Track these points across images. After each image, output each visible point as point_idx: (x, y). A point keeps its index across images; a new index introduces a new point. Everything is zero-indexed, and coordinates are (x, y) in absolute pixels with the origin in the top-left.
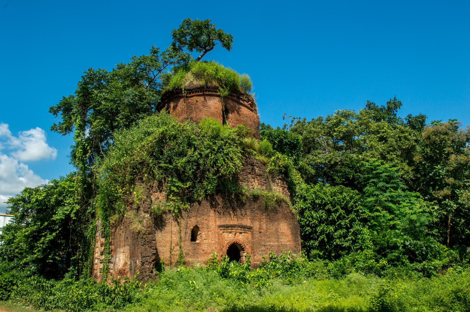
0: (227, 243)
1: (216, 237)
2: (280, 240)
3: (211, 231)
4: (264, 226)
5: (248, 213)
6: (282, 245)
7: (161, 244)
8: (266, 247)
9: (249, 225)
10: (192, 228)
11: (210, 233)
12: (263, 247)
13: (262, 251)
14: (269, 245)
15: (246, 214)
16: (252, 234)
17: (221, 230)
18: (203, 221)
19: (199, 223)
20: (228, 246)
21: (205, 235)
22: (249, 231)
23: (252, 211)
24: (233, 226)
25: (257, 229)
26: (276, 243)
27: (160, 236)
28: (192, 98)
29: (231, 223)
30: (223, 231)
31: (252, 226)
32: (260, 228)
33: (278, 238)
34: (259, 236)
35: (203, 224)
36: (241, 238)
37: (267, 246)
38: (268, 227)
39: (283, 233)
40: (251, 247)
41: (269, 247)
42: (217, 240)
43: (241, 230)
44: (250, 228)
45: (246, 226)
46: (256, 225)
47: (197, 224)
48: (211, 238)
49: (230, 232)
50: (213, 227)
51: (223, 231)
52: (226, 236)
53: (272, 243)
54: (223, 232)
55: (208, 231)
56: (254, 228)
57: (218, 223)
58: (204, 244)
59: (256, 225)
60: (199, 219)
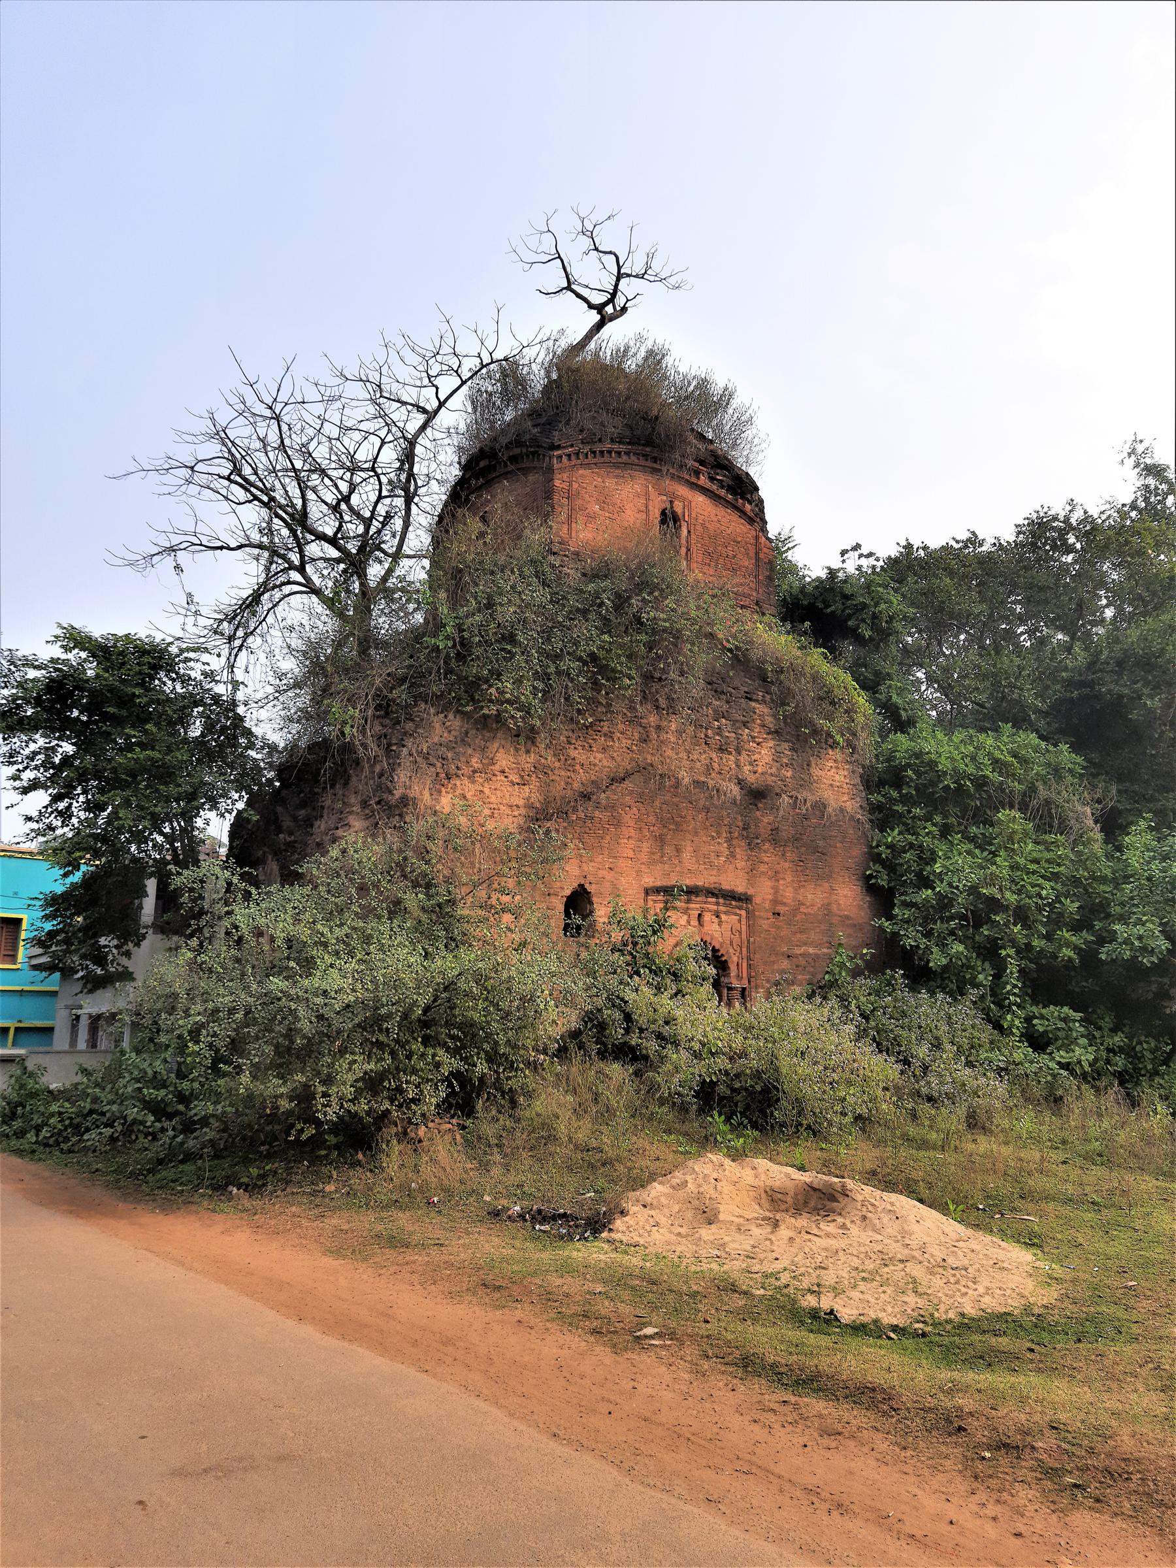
9: (740, 889)
10: (568, 892)
15: (732, 855)
17: (655, 901)
18: (601, 873)
19: (590, 878)
24: (692, 891)
26: (825, 950)
32: (775, 902)
37: (796, 956)
40: (749, 959)
41: (802, 961)
43: (717, 904)
45: (733, 891)
46: (762, 893)
49: (686, 911)
50: (630, 892)
53: (811, 950)
56: (757, 900)
57: (649, 881)
60: (589, 868)
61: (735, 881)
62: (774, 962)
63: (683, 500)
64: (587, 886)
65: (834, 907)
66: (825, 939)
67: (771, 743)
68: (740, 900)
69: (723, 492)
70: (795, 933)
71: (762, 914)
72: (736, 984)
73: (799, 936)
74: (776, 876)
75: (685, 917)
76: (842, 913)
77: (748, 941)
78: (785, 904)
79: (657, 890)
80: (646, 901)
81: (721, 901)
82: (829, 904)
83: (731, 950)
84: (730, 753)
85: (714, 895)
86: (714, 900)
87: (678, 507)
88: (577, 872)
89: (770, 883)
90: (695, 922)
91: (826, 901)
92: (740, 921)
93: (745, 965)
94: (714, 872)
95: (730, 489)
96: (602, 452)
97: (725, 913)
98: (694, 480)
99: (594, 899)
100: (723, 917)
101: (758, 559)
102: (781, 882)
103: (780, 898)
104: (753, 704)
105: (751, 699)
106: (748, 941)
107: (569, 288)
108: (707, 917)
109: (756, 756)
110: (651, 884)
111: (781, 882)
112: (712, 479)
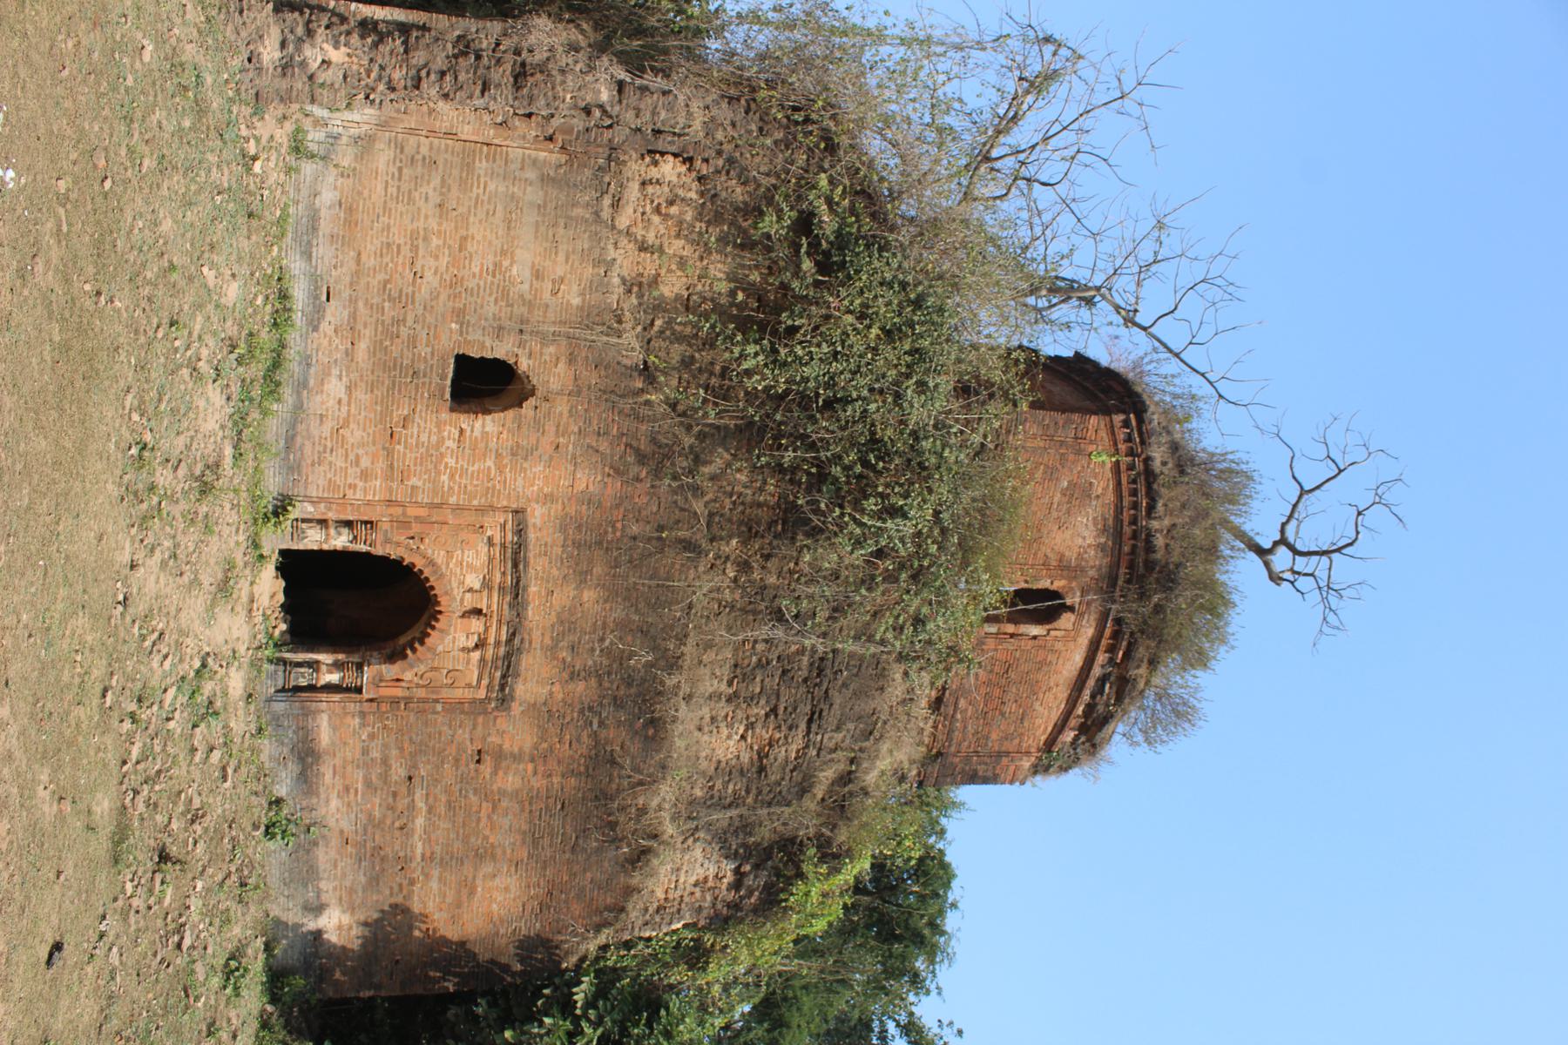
0: (432, 563)
1: (473, 496)
2: (436, 873)
3: (501, 470)
4: (510, 781)
5: (580, 686)
6: (412, 882)
7: (455, 192)
8: (404, 790)
10: (524, 365)
11: (490, 463)
12: (403, 773)
13: (385, 762)
14: (412, 806)
15: (574, 676)
16: (477, 708)
18: (550, 428)
19: (545, 406)
20: (420, 564)
21: (485, 434)
22: (489, 687)
23: (589, 709)
24: (516, 592)
25: (494, 739)
26: (419, 851)
27: (492, 187)
28: (1103, 434)
29: (533, 589)
30: (497, 540)
31: (517, 709)
32: (499, 755)
33: (449, 861)
34: (461, 749)
35: (538, 426)
36: (454, 644)
37: (410, 792)
38: (505, 803)
39: (472, 892)
40: (408, 701)
41: (402, 803)
42: (453, 500)
43: (497, 643)
44: (504, 696)
47: (539, 393)
48: (464, 472)
49: (487, 584)
50: (520, 482)
51: (497, 540)
52: (469, 556)
53: (420, 822)
54: (490, 539)
55: (498, 455)
56: (502, 723)
57: (537, 515)
58: (439, 425)
59: (515, 732)
60: (562, 407)
61: (536, 681)
62: (401, 749)
63: (1077, 627)
64: (532, 401)
65: (488, 868)
66: (438, 849)
67: (745, 758)
68: (502, 687)
69: (1086, 696)
70: (448, 791)
71: (480, 728)
72: (368, 673)
73: (443, 798)
74: (539, 757)
75: (477, 586)
76: (479, 882)
77: (437, 701)
78: (495, 773)
79: (520, 531)
80: (505, 509)
81: (502, 651)
82: (493, 857)
83: (422, 668)
84: (730, 683)
85: (509, 641)
86: (504, 638)
87: (1066, 620)
88: (555, 385)
89: (527, 746)
90: (469, 601)
91: (499, 851)
92: (469, 686)
93: (399, 692)
94: (548, 641)
95: (1090, 708)
96: (1134, 493)
97: (482, 660)
98: (1104, 642)
99: (510, 414)
100: (476, 655)
101: (1000, 755)
102: (530, 767)
103: (504, 764)
104: (803, 726)
105: (810, 721)
106: (437, 701)
107: (1303, 492)
108: (476, 625)
109: (725, 732)
110: (531, 521)
111: (530, 767)
112: (1102, 680)
